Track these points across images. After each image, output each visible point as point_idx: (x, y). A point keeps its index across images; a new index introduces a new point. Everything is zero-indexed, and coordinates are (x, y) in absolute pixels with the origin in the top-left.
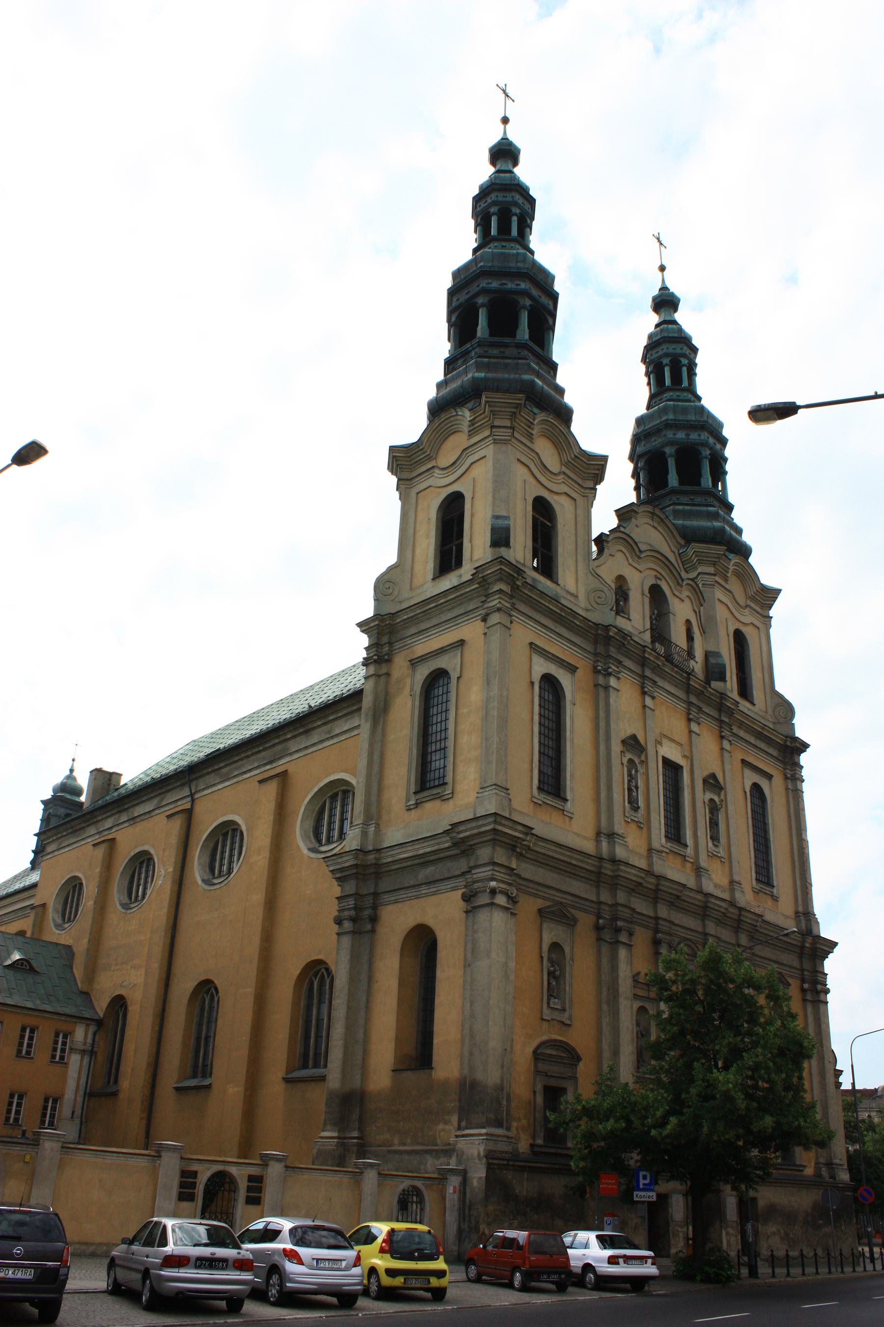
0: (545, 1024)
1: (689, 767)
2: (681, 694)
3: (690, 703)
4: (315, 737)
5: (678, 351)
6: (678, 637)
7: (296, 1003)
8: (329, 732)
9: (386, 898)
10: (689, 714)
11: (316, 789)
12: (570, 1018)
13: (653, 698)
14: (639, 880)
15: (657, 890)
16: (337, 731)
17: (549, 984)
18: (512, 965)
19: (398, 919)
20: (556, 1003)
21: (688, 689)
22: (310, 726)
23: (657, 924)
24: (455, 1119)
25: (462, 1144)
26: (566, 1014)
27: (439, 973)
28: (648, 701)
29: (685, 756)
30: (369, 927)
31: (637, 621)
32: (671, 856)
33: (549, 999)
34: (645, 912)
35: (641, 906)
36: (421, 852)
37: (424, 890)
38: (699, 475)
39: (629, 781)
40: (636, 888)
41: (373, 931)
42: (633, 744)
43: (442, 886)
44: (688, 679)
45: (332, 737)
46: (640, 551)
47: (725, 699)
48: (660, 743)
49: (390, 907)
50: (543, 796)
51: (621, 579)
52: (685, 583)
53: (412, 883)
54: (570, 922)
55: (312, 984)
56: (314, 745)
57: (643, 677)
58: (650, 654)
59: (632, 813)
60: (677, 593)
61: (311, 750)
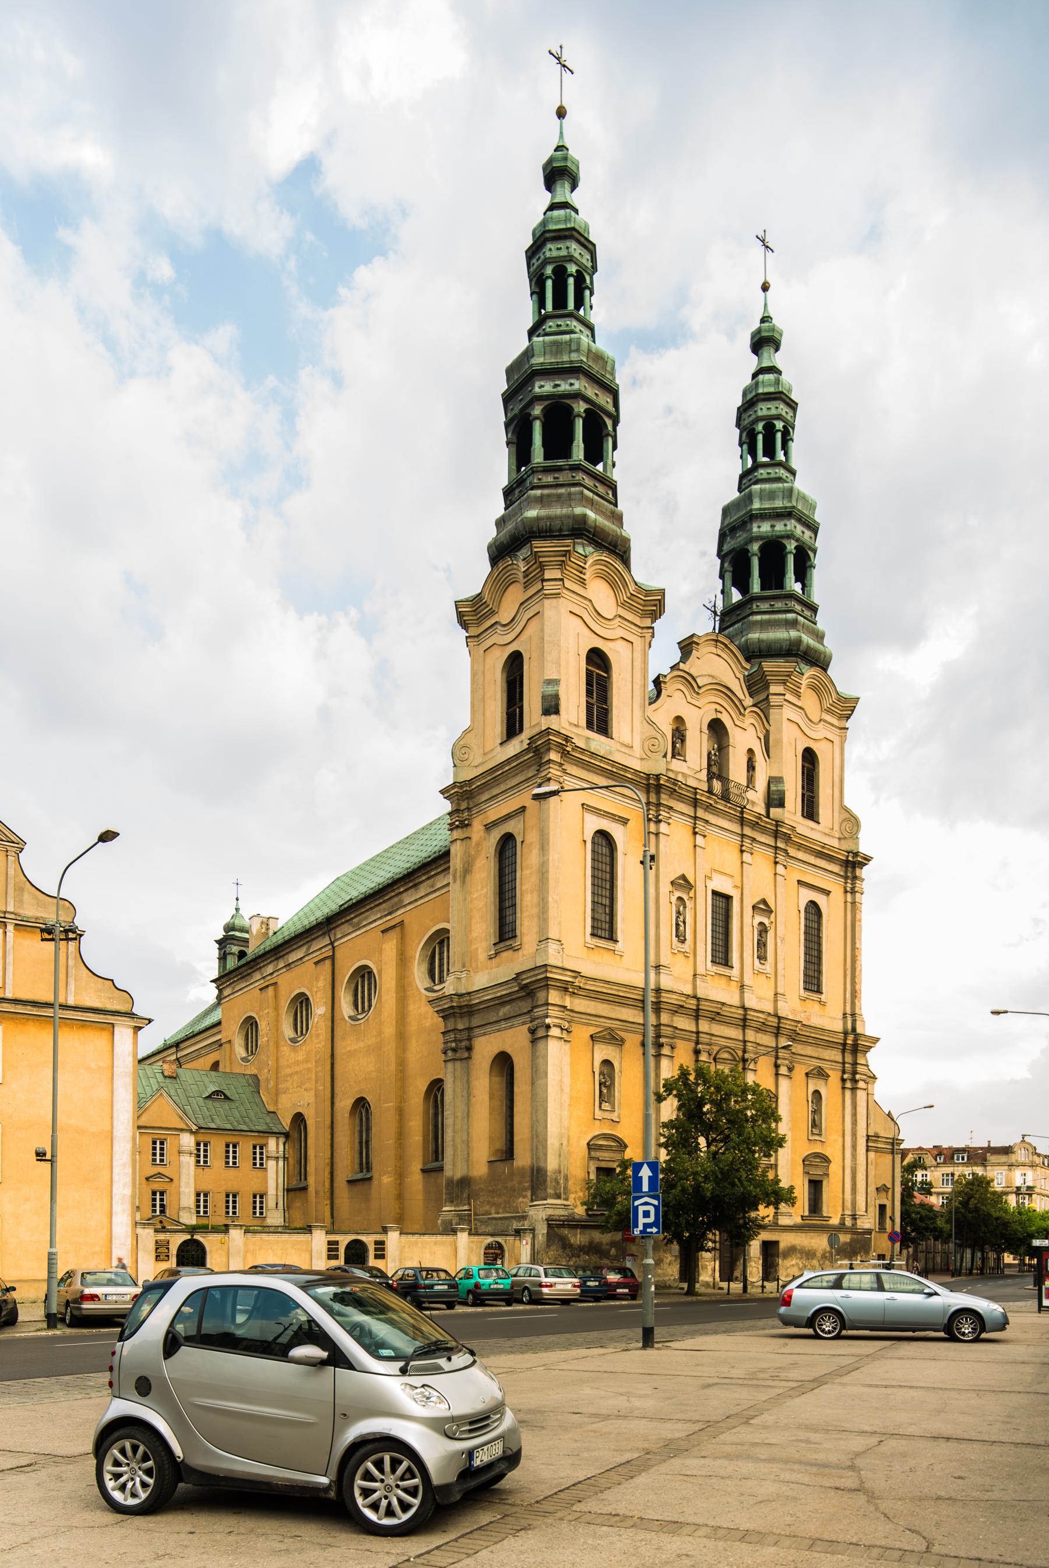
0: (598, 1122)
1: (739, 896)
2: (736, 828)
3: (743, 836)
4: (422, 891)
5: (773, 412)
6: (737, 772)
7: (426, 1112)
8: (432, 886)
9: (477, 1031)
10: (742, 846)
11: (430, 933)
12: (619, 1117)
13: (705, 836)
14: (681, 1003)
15: (697, 1010)
16: (439, 886)
17: (601, 1091)
18: (567, 1080)
19: (486, 1047)
20: (606, 1106)
21: (742, 821)
22: (417, 881)
23: (698, 1037)
24: (529, 1194)
25: (532, 1212)
26: (616, 1114)
27: (515, 1089)
28: (699, 840)
29: (736, 887)
30: (466, 1055)
31: (692, 768)
32: (716, 977)
33: (600, 1104)
34: (687, 1028)
35: (684, 1023)
36: (499, 994)
37: (503, 1025)
38: (782, 574)
39: (677, 917)
40: (678, 1009)
41: (469, 1058)
42: (683, 883)
43: (516, 1021)
44: (742, 812)
45: (435, 891)
46: (699, 687)
47: (781, 826)
48: (710, 878)
49: (481, 1038)
50: (597, 942)
51: (679, 720)
52: (748, 711)
53: (495, 1019)
54: (619, 1042)
55: (436, 1096)
56: (421, 898)
57: (695, 818)
58: (702, 795)
59: (679, 944)
60: (737, 723)
61: (419, 903)
